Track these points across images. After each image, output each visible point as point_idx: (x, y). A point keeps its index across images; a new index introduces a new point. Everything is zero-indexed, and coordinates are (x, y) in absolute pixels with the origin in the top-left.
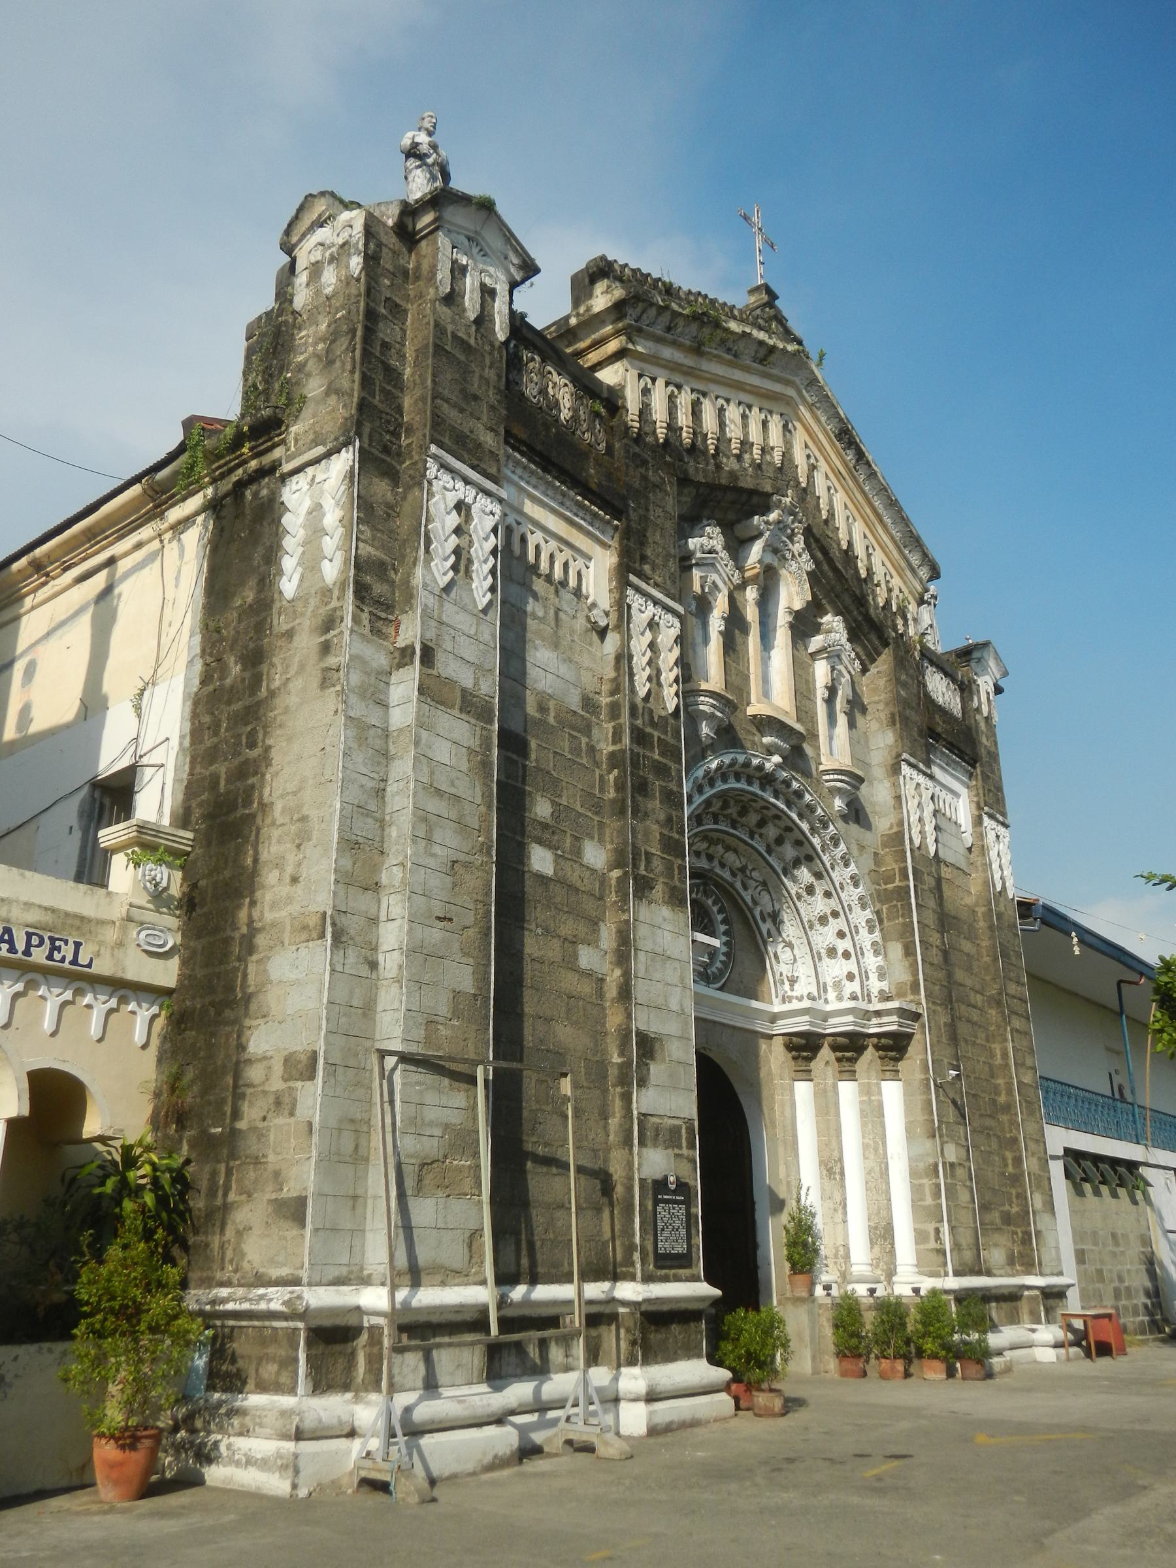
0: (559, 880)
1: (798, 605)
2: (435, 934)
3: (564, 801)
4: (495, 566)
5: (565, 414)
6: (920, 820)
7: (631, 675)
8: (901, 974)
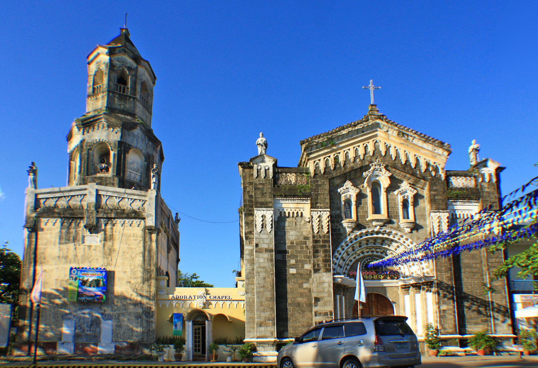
0: (297, 273)
1: (386, 186)
2: (262, 289)
3: (299, 259)
4: (272, 223)
5: (293, 182)
6: (439, 226)
7: (313, 230)
8: (431, 267)
